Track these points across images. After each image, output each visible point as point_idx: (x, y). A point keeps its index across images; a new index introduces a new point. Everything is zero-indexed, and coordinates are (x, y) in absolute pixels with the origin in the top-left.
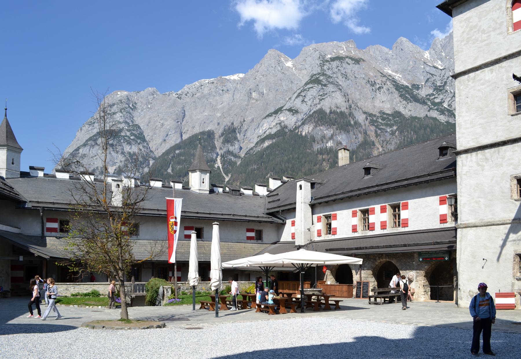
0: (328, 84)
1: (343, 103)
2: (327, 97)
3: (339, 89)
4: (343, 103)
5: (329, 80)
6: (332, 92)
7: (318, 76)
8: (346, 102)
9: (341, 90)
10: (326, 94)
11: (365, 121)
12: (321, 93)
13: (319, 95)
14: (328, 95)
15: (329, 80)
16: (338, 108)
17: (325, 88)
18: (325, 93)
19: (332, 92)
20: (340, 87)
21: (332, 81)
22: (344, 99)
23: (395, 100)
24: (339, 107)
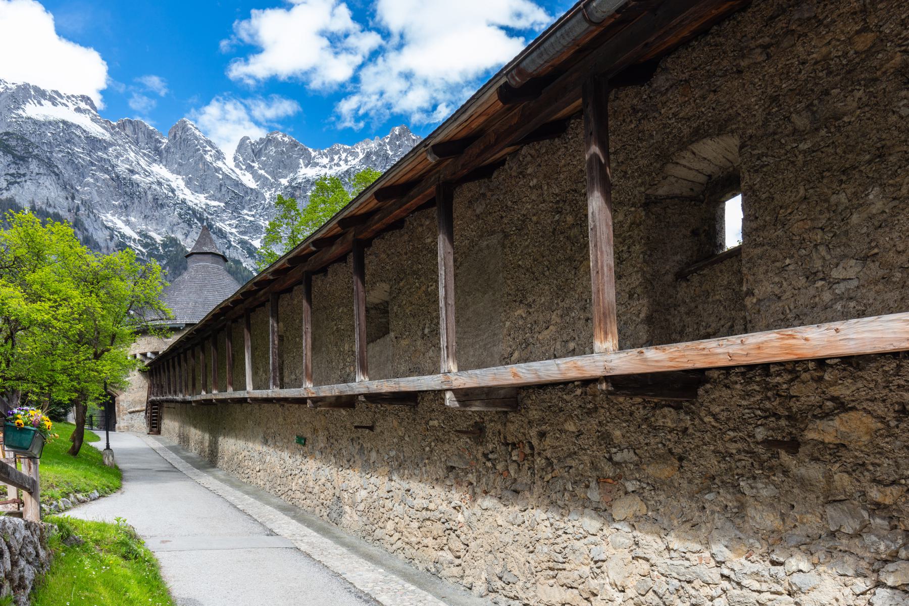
0: (28, 158)
1: (61, 200)
2: (26, 181)
3: (54, 172)
4: (61, 200)
5: (31, 150)
6: (37, 174)
7: (5, 138)
8: (67, 198)
9: (57, 175)
10: (24, 175)
11: (109, 241)
12: (12, 171)
13: (6, 172)
14: (27, 177)
15: (31, 150)
16: (50, 206)
17: (21, 162)
18: (22, 172)
19: (37, 174)
20: (56, 170)
21: (37, 154)
22: (63, 194)
23: (167, 217)
24: (53, 205)
